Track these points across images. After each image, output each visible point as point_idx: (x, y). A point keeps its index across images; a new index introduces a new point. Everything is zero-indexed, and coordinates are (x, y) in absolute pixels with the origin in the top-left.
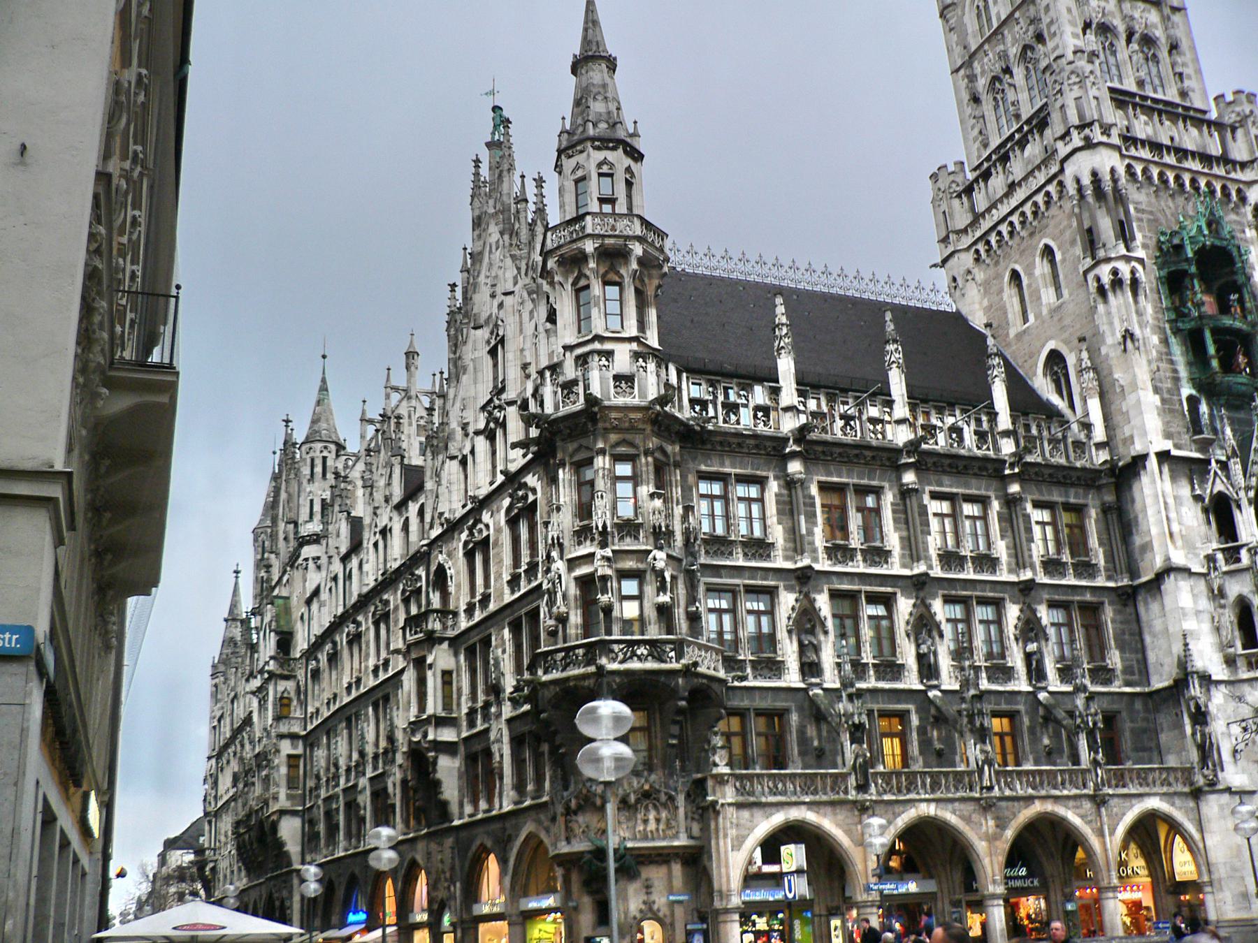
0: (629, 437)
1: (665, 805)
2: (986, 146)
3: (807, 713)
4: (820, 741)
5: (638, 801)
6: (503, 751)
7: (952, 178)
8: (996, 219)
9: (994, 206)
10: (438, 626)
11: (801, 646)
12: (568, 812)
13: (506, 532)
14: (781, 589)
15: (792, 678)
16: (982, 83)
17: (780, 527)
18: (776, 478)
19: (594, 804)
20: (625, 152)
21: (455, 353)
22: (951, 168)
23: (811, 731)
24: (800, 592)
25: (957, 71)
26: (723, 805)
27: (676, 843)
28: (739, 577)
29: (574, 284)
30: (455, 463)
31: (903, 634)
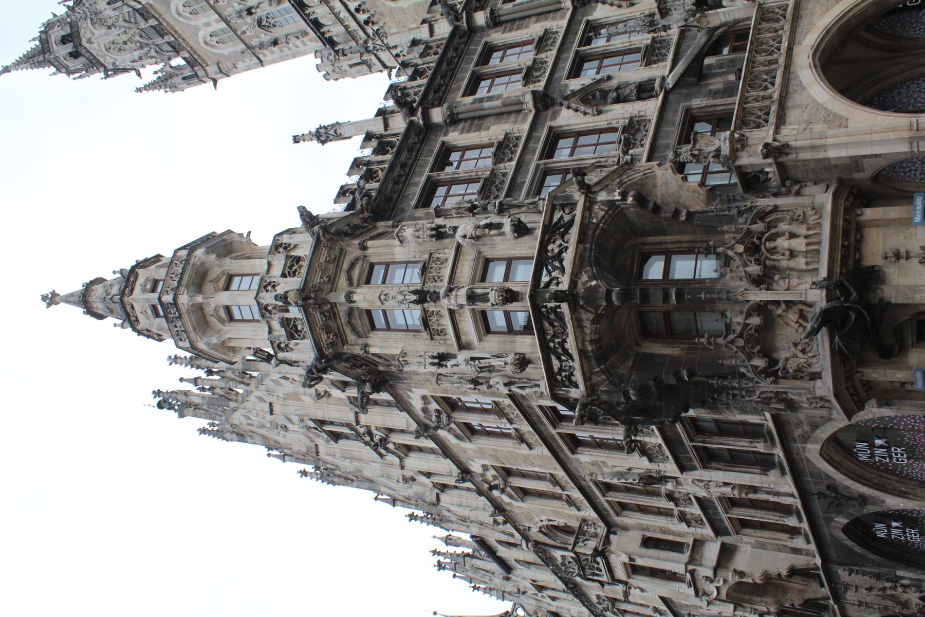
0: (345, 266)
1: (769, 226)
2: (306, 34)
3: (695, 90)
4: (731, 73)
5: (758, 262)
6: (717, 482)
7: (325, 60)
8: (347, 14)
9: (341, 21)
10: (592, 544)
11: (617, 101)
12: (772, 371)
13: (482, 443)
14: (553, 124)
15: (650, 108)
16: (265, 37)
17: (492, 128)
18: (446, 134)
19: (758, 329)
20: (142, 267)
21: (353, 481)
22: (319, 61)
23: (716, 84)
24: (561, 105)
25: (261, 61)
26: (775, 140)
27: (829, 207)
28: (528, 165)
29: (223, 322)
30: (444, 497)
31: (631, 9)
